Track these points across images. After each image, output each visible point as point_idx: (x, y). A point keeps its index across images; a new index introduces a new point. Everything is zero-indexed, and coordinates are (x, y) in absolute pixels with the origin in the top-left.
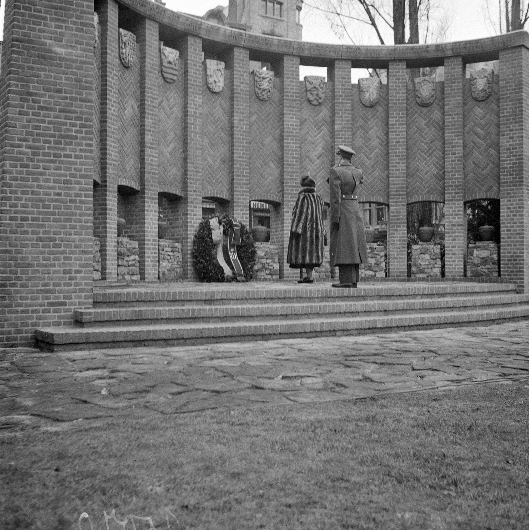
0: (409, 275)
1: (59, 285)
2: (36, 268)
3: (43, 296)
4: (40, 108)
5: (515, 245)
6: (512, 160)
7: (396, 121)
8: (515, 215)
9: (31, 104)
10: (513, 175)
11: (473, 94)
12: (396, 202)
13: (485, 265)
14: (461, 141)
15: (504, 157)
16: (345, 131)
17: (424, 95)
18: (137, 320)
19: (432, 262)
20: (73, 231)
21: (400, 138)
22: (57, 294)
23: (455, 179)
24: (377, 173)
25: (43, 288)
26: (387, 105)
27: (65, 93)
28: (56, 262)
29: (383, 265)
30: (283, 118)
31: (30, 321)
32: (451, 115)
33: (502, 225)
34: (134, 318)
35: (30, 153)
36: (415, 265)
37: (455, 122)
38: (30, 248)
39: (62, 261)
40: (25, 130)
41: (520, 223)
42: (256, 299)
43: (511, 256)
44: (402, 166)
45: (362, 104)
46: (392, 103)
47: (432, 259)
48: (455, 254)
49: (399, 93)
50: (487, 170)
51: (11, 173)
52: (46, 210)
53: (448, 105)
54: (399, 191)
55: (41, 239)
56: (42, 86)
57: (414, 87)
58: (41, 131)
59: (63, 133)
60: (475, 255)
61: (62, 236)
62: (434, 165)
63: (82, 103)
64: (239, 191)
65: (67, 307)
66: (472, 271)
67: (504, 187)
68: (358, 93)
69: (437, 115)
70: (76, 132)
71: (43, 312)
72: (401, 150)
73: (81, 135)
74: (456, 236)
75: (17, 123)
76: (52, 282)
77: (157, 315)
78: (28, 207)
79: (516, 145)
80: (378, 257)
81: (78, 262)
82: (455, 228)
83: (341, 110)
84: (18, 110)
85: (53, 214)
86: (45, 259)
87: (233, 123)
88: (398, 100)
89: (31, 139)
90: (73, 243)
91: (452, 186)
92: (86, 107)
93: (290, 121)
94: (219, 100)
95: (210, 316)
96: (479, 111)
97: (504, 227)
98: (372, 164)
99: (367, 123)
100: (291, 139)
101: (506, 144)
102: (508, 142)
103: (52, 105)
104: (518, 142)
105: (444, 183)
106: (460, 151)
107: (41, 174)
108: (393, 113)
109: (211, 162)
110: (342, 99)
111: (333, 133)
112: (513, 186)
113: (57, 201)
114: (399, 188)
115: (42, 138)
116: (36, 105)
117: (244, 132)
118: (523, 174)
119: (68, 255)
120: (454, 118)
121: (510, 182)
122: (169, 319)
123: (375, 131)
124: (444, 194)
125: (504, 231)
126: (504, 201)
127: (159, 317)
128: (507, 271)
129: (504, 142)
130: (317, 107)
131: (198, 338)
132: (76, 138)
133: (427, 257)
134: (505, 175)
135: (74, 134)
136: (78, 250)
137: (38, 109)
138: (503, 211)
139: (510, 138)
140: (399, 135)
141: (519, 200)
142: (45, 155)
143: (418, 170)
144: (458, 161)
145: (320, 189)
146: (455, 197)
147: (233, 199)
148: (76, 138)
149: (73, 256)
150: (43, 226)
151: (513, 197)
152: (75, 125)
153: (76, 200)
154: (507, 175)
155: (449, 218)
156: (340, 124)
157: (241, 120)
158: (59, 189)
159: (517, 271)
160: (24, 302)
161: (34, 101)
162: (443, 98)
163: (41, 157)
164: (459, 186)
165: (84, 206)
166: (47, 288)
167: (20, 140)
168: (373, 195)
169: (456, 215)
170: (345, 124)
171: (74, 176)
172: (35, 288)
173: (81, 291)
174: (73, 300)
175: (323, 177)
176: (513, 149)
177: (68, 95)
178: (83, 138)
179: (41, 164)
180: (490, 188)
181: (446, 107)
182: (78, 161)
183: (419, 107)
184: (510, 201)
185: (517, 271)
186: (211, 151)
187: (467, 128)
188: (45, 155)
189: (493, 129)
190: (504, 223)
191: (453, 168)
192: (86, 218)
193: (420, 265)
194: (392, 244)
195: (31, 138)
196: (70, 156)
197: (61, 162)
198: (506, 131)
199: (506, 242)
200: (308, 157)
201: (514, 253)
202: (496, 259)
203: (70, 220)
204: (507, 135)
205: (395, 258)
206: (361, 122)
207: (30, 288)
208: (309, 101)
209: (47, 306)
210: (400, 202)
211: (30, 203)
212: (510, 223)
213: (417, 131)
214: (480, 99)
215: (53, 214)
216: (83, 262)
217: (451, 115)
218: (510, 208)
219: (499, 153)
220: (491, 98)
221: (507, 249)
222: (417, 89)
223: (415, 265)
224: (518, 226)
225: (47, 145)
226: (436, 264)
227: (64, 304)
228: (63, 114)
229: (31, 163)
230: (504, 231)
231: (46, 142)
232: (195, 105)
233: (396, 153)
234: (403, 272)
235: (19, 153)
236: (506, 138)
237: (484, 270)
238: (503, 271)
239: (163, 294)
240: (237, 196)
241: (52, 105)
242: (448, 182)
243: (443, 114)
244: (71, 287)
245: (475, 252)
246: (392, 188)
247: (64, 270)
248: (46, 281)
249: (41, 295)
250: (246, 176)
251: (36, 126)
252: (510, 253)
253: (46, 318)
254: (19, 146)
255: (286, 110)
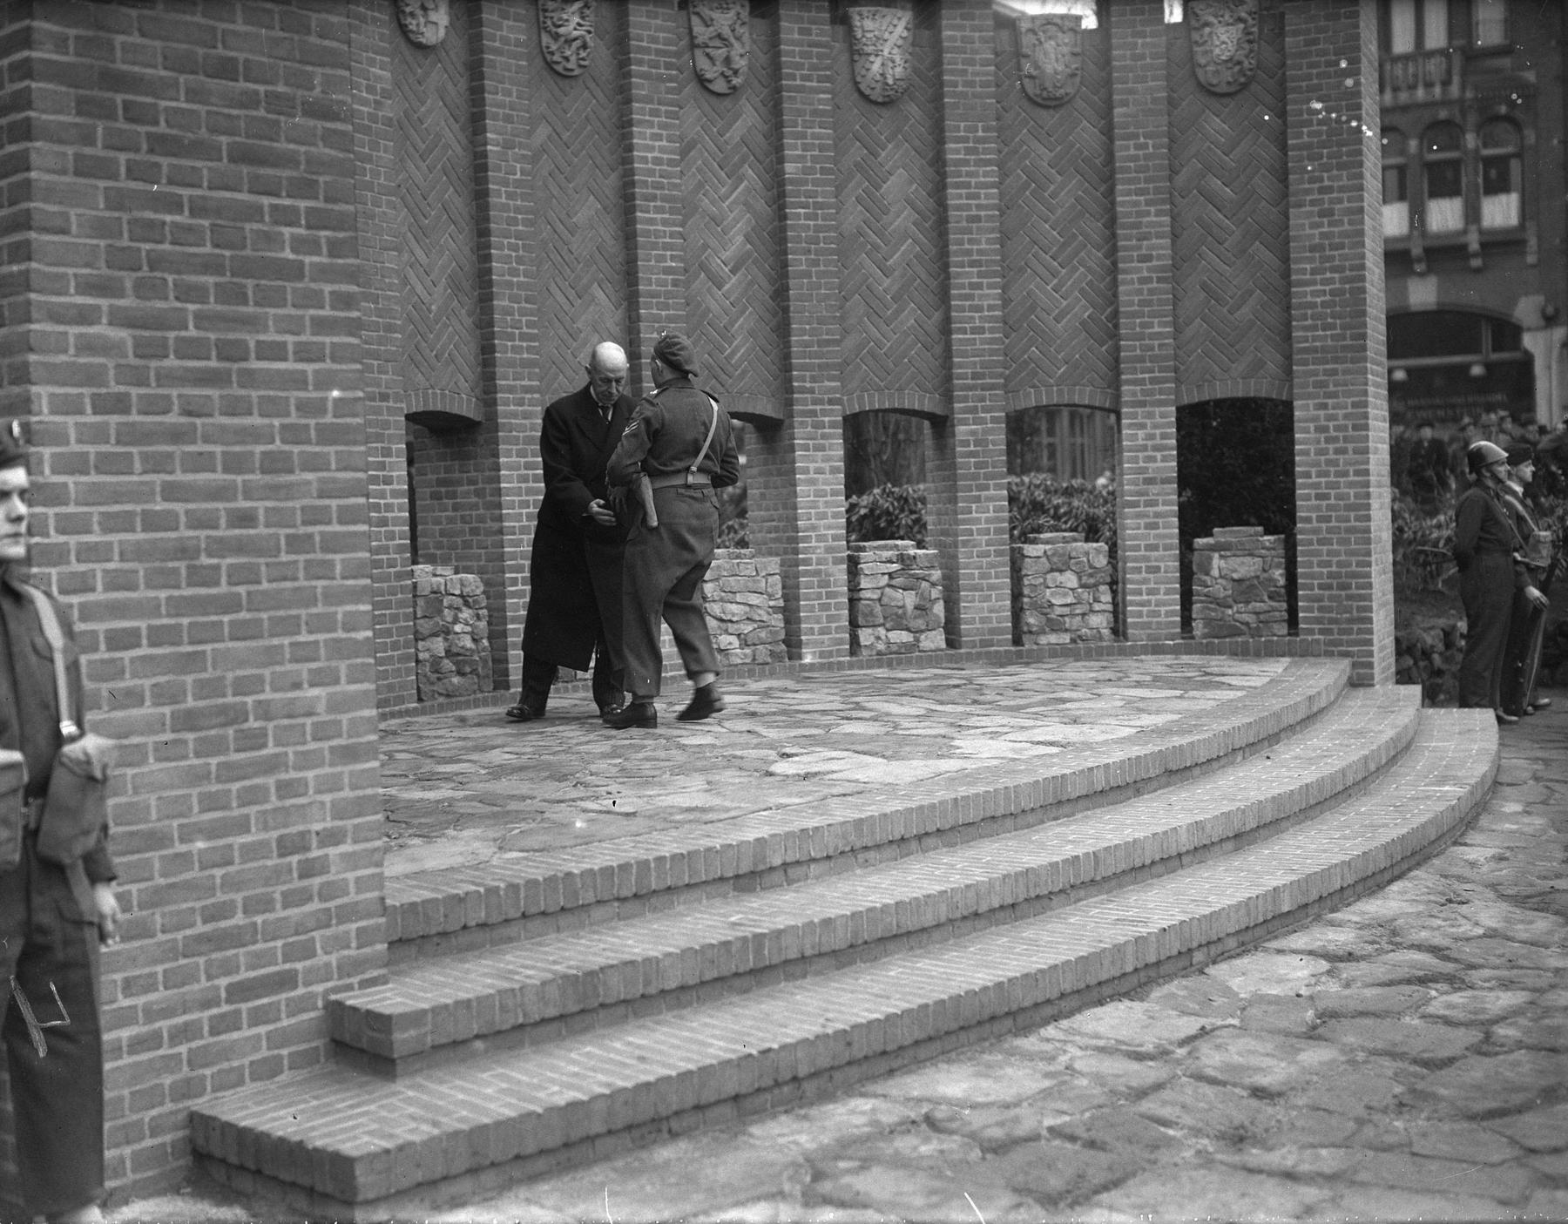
0: (1017, 641)
1: (266, 904)
2: (181, 848)
3: (209, 964)
4: (159, 144)
5: (1341, 542)
6: (1331, 281)
7: (968, 151)
8: (1343, 451)
9: (121, 124)
10: (1332, 327)
11: (1200, 72)
12: (974, 410)
13: (1247, 602)
14: (1167, 219)
15: (1304, 271)
16: (816, 183)
17: (1049, 69)
18: (582, 1011)
19: (1086, 595)
20: (304, 668)
21: (979, 207)
22: (259, 946)
23: (1153, 336)
24: (910, 317)
25: (209, 927)
26: (938, 98)
27: (247, 80)
28: (252, 810)
29: (939, 609)
30: (630, 135)
31: (167, 1080)
32: (1136, 136)
33: (1299, 481)
34: (573, 1007)
35: (130, 343)
36: (1036, 607)
37: (1146, 157)
38: (153, 765)
39: (274, 802)
40: (102, 243)
41: (1357, 473)
42: (878, 847)
43: (1331, 575)
44: (990, 295)
45: (861, 93)
46: (954, 95)
47: (1082, 586)
48: (1157, 569)
49: (972, 62)
50: (1245, 312)
51: (59, 438)
52: (203, 591)
53: (1125, 104)
54: (983, 376)
55: (187, 721)
56: (158, 43)
57: (1016, 42)
58: (166, 247)
59: (248, 252)
60: (1215, 573)
61: (268, 695)
62: (1082, 291)
63: (311, 122)
64: (511, 390)
65: (301, 991)
66: (1208, 622)
67: (1305, 363)
68: (845, 57)
69: (1087, 134)
70: (299, 245)
71: (214, 1032)
72: (983, 246)
73: (316, 259)
74: (1157, 515)
75: (73, 213)
76: (239, 897)
77: (647, 983)
78: (133, 587)
79: (1341, 234)
80: (924, 584)
81: (327, 798)
82: (1154, 489)
83: (800, 113)
84: (70, 151)
85: (231, 604)
86: (211, 802)
87: (484, 155)
88: (971, 84)
89: (128, 284)
90: (309, 721)
91: (1141, 360)
92: (329, 137)
93: (651, 145)
94: (437, 77)
95: (808, 952)
96: (1216, 125)
97: (1305, 486)
98: (896, 287)
99: (876, 156)
100: (658, 210)
101: (1308, 231)
102: (1313, 226)
103: (203, 133)
104: (1347, 227)
105: (1118, 349)
106: (1161, 247)
107: (177, 435)
108: (956, 126)
109: (419, 288)
110: (804, 78)
111: (777, 192)
112: (1336, 360)
113: (240, 547)
114: (983, 365)
115: (170, 278)
116: (142, 129)
117: (518, 183)
118: (1364, 325)
119: (293, 775)
120: (1145, 146)
121: (1324, 349)
122: (683, 988)
123: (901, 183)
124: (1115, 383)
125: (1307, 498)
126: (1306, 407)
127: (652, 990)
128: (1318, 621)
129: (1304, 226)
130: (727, 102)
131: (839, 1067)
132: (296, 272)
133: (1070, 579)
134: (1305, 328)
135: (288, 254)
136: (326, 745)
137: (151, 151)
138: (1304, 439)
139: (1322, 214)
140: (977, 196)
141: (1354, 405)
142: (189, 349)
143: (1032, 309)
144: (1159, 280)
145: (744, 372)
146: (1151, 393)
147: (492, 416)
148: (296, 272)
149: (310, 774)
150: (192, 662)
151: (1334, 395)
152: (286, 217)
153: (310, 536)
154: (1315, 328)
155: (1135, 460)
156: (801, 159)
157: (508, 145)
158: (248, 496)
159: (1351, 621)
160: (140, 1001)
161: (134, 114)
162: (1108, 82)
163: (172, 362)
164: (1166, 358)
165: (338, 557)
166: (223, 924)
167: (87, 287)
168: (900, 389)
169: (1156, 448)
170: (814, 159)
171: (294, 434)
172: (179, 936)
173: (345, 914)
174: (321, 959)
175: (751, 333)
176: (1333, 247)
177: (261, 88)
178: (323, 273)
179: (174, 393)
180: (1259, 365)
181: (1117, 111)
182: (309, 368)
183: (1026, 103)
184: (1324, 406)
185: (1351, 621)
186: (419, 253)
187: (1180, 180)
188: (189, 349)
189: (1263, 183)
190: (1307, 475)
191: (1142, 303)
192: (349, 608)
193: (1051, 605)
194: (965, 544)
195: (128, 279)
196: (275, 352)
197: (249, 378)
198: (1308, 192)
199: (1316, 531)
200: (702, 267)
201: (1339, 564)
202: (1282, 582)
203: (292, 626)
204: (1313, 203)
205: (975, 588)
206: (856, 152)
207: (161, 937)
208: (702, 82)
209: (228, 1001)
210: (985, 410)
211: (141, 568)
212: (1327, 474)
213: (1026, 186)
214: (1224, 89)
215: (231, 604)
216: (347, 793)
217: (1136, 136)
218: (1325, 429)
219: (1286, 260)
220: (1254, 87)
221: (1318, 553)
222: (1025, 50)
223: (1036, 607)
224: (1351, 485)
225: (191, 307)
226: (1096, 600)
227: (286, 981)
228: (245, 170)
229: (134, 391)
230: (1307, 498)
231: (187, 293)
232: (371, 89)
233: (969, 252)
234: (1001, 631)
235: (88, 346)
236: (1310, 214)
237: (1246, 617)
238: (1307, 620)
239: (607, 872)
240: (506, 407)
241: (203, 133)
242: (1130, 348)
243: (1108, 132)
244: (308, 908)
245: (1217, 562)
246: (961, 366)
247: (280, 840)
248: (221, 897)
249: (201, 960)
250: (531, 338)
251: (151, 224)
252: (1329, 564)
253: (226, 1052)
254: (85, 316)
255: (639, 111)
